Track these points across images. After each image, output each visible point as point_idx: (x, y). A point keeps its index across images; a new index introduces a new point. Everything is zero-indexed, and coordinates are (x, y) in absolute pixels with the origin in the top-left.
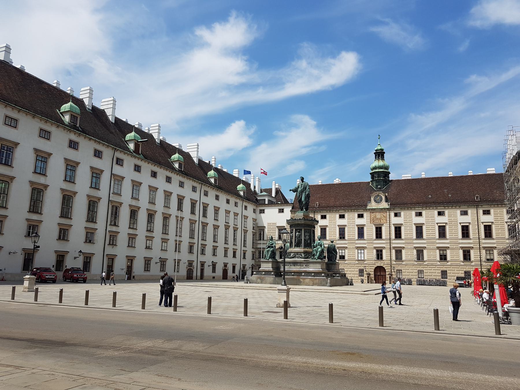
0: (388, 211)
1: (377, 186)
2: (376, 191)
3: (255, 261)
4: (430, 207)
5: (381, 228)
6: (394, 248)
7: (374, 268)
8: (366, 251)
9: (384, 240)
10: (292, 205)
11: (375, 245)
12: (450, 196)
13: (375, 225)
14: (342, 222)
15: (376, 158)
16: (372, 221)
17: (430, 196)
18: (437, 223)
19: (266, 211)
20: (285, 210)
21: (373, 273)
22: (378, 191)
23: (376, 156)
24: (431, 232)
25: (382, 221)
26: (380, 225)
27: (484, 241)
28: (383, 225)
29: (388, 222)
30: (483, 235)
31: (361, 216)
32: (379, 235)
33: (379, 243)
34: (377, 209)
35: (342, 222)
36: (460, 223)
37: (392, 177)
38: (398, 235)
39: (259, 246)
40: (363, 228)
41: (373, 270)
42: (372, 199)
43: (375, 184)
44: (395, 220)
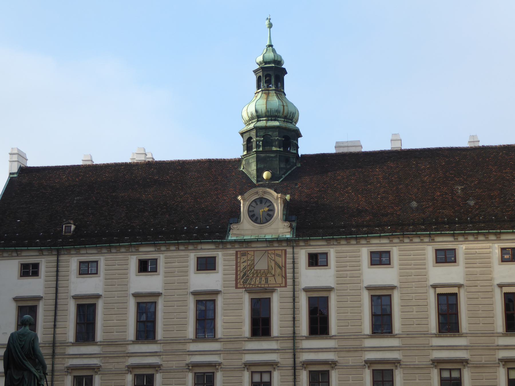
0: (289, 250)
1: (259, 172)
2: (255, 186)
4: (410, 237)
5: (268, 302)
6: (306, 364)
9: (276, 339)
12: (472, 203)
13: (249, 291)
15: (259, 87)
16: (243, 279)
17: (414, 204)
18: (434, 287)
22: (260, 186)
23: (259, 80)
25: (271, 280)
26: (266, 290)
28: (272, 291)
29: (290, 281)
31: (206, 265)
32: (261, 326)
33: (262, 350)
34: (257, 241)
36: (501, 286)
37: (306, 147)
38: (319, 325)
40: (214, 301)
42: (243, 208)
43: (253, 167)
44: (311, 278)
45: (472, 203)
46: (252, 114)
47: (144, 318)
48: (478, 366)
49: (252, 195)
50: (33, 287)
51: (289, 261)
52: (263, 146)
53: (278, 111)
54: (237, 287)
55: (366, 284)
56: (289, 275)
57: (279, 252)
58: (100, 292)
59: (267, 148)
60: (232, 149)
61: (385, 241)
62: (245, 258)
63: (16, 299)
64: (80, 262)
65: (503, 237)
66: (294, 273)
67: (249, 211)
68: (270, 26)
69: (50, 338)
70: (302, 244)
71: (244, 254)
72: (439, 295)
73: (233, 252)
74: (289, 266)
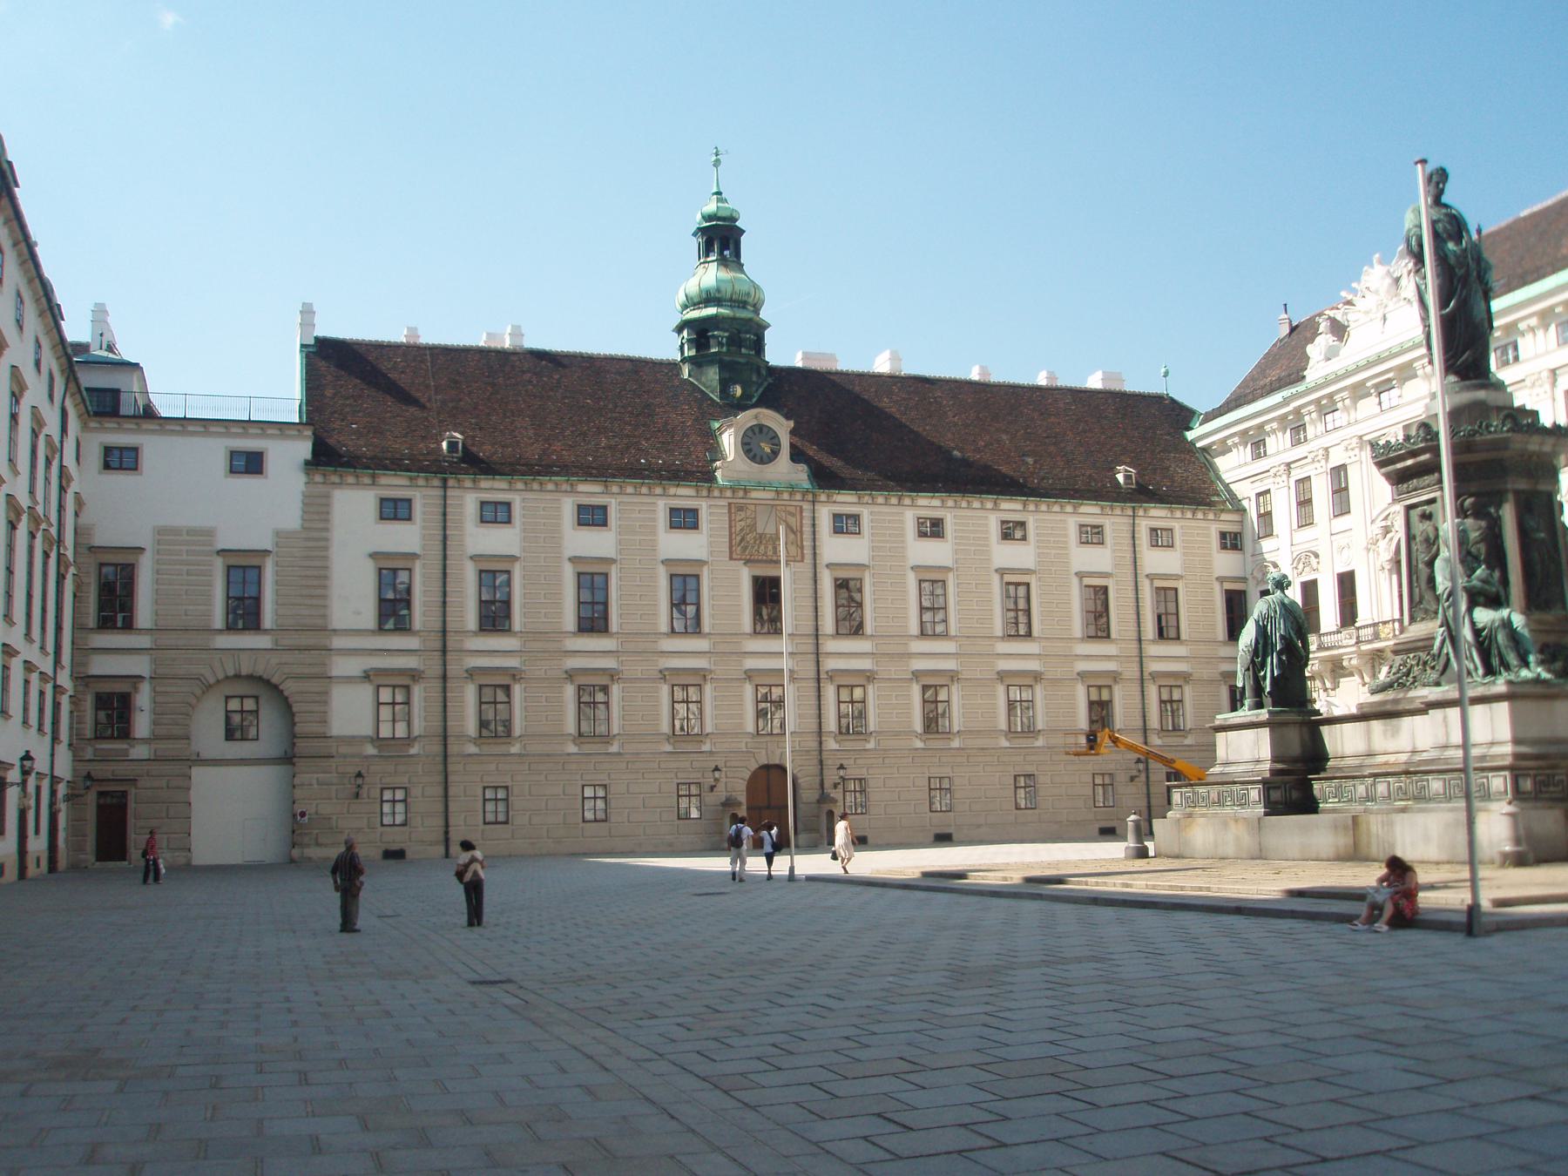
0: (806, 506)
1: (725, 385)
3: (77, 759)
7: (747, 775)
8: (708, 688)
10: (309, 432)
11: (751, 663)
14: (596, 543)
19: (148, 458)
20: (271, 463)
21: (743, 798)
24: (977, 608)
27: (1153, 649)
29: (808, 551)
30: (1150, 629)
31: (684, 520)
35: (596, 543)
39: (101, 666)
41: (742, 786)
43: (712, 375)
44: (837, 549)
45: (1030, 460)
46: (708, 292)
47: (586, 596)
48: (1055, 682)
49: (746, 418)
50: (404, 537)
51: (807, 522)
52: (728, 345)
53: (748, 294)
54: (731, 558)
55: (912, 562)
56: (807, 543)
57: (792, 509)
58: (515, 551)
59: (733, 349)
60: (666, 346)
61: (936, 502)
62: (743, 514)
63: (374, 556)
64: (482, 503)
65: (1083, 509)
66: (814, 540)
67: (744, 444)
68: (717, 163)
69: (438, 626)
70: (823, 498)
71: (741, 508)
72: (1008, 584)
73: (724, 502)
74: (807, 529)
